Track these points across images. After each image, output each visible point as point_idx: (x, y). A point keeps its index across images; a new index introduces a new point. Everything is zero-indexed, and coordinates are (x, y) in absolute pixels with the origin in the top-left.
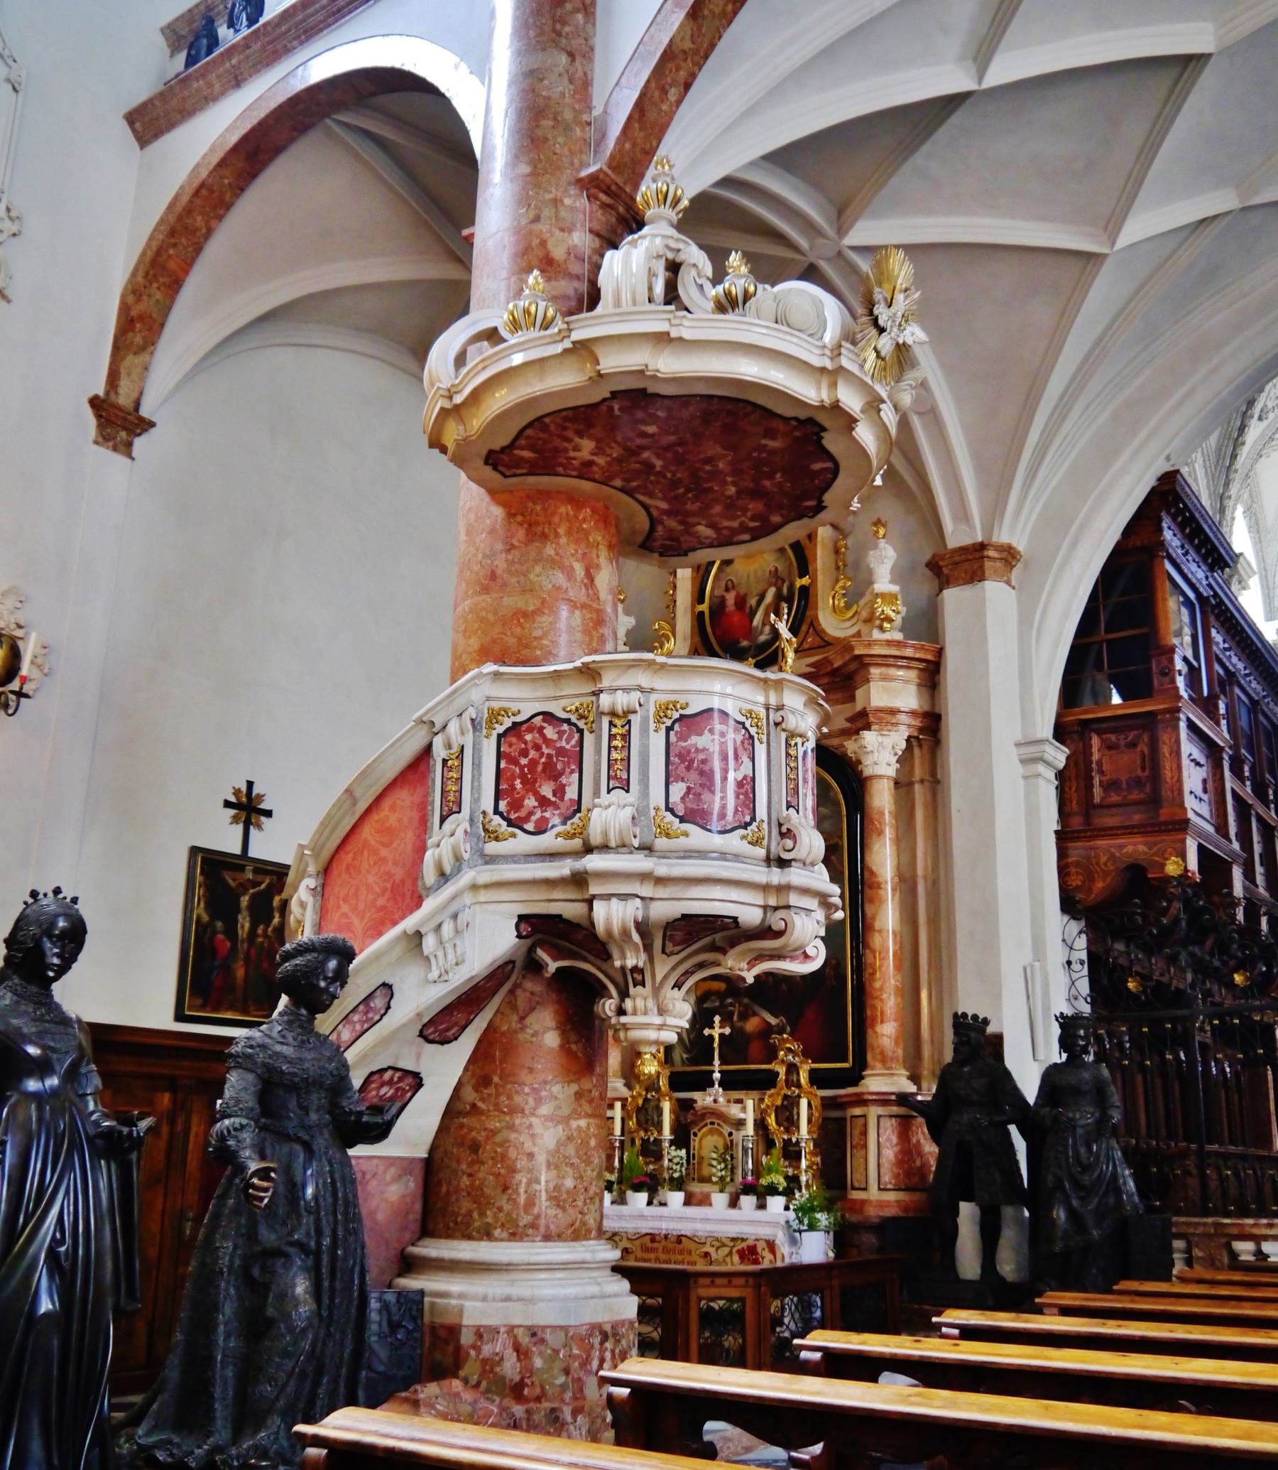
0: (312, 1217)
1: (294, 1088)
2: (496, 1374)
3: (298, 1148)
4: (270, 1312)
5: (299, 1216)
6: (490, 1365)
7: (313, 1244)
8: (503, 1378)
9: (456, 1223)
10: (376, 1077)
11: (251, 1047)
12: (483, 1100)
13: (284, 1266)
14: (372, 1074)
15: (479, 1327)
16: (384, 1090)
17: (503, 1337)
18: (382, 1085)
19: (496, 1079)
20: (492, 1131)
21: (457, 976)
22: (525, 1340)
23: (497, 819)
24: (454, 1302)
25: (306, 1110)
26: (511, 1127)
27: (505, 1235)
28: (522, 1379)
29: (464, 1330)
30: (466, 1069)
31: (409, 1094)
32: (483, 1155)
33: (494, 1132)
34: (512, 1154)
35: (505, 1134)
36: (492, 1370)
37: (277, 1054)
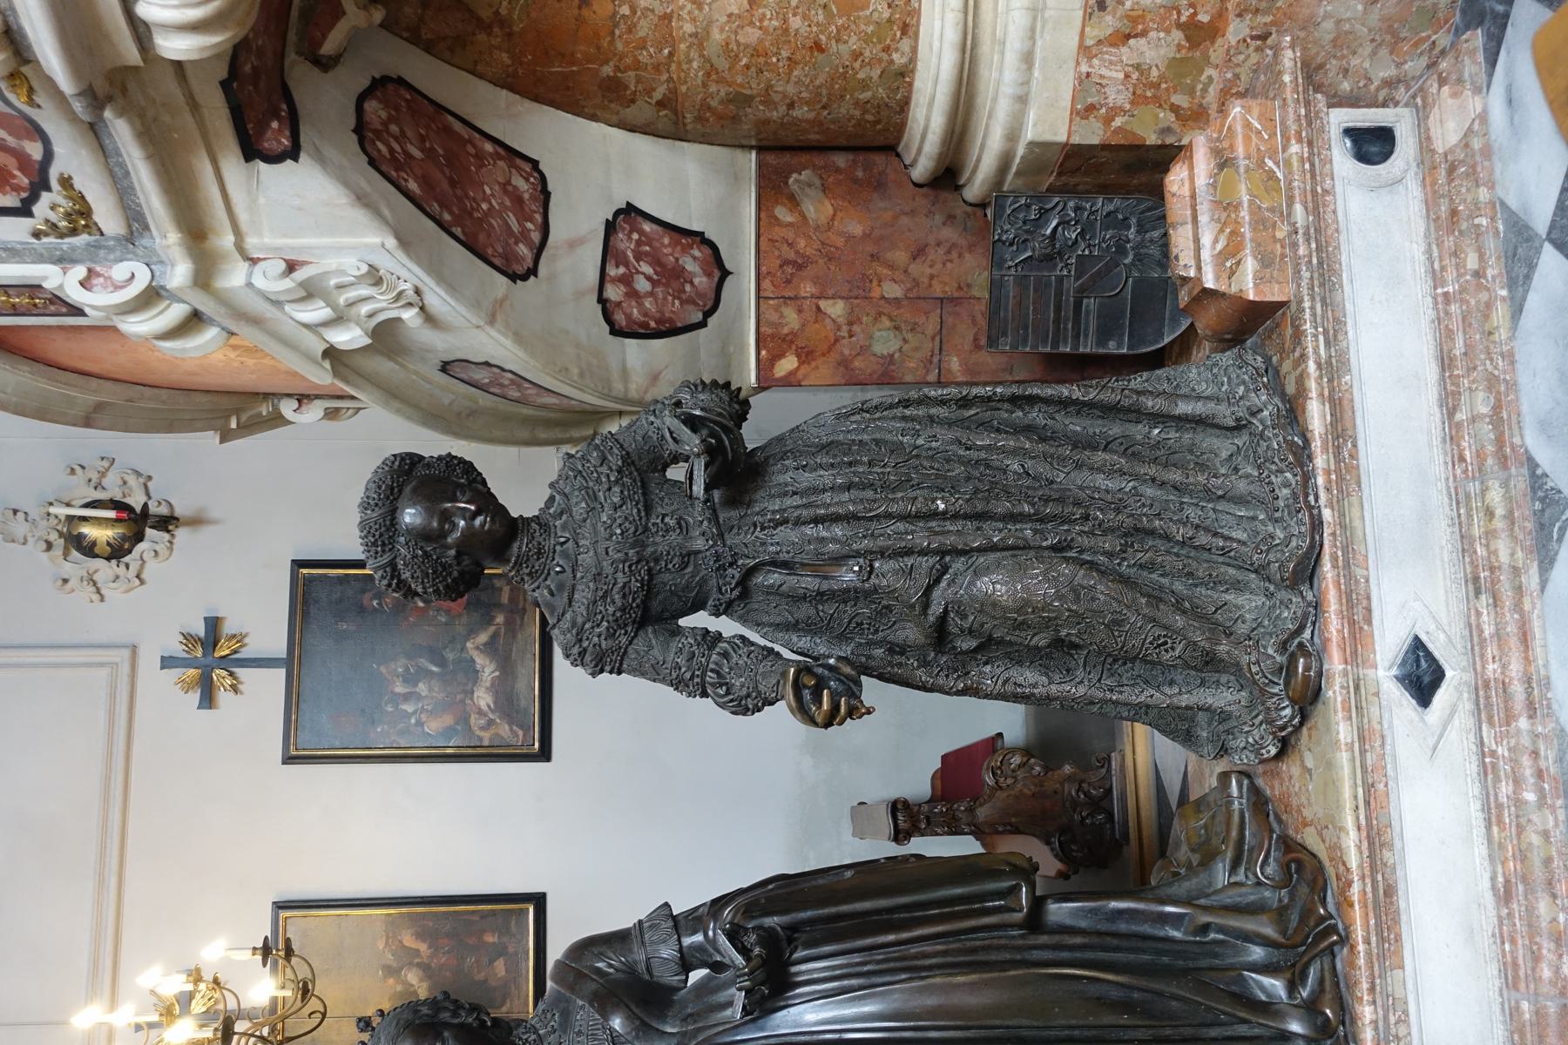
0: (877, 565)
1: (649, 586)
2: (1162, 77)
3: (759, 579)
4: (1041, 640)
5: (875, 590)
6: (1146, 91)
7: (926, 562)
8: (1174, 63)
9: (878, 122)
10: (620, 318)
11: (582, 653)
12: (649, 91)
13: (964, 617)
14: (616, 331)
15: (1074, 112)
16: (642, 285)
17: (1098, 67)
18: (633, 294)
19: (608, 70)
20: (708, 74)
21: (404, 274)
22: (1109, 23)
23: (41, 208)
24: (1021, 151)
25: (688, 556)
26: (700, 39)
27: (905, 45)
28: (1179, 26)
29: (1076, 140)
30: (593, 118)
31: (647, 227)
32: (756, 87)
33: (711, 71)
34: (751, 35)
35: (712, 49)
36: (1156, 86)
37: (591, 614)
